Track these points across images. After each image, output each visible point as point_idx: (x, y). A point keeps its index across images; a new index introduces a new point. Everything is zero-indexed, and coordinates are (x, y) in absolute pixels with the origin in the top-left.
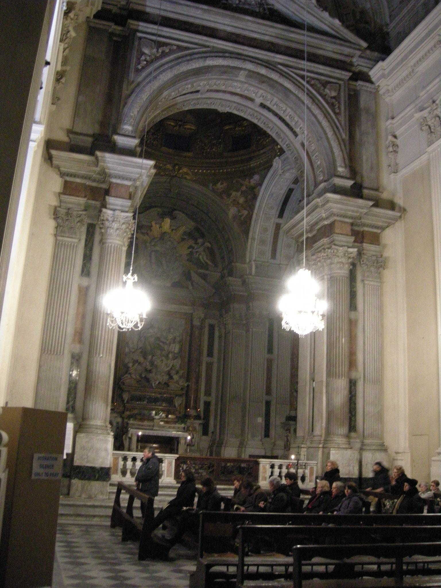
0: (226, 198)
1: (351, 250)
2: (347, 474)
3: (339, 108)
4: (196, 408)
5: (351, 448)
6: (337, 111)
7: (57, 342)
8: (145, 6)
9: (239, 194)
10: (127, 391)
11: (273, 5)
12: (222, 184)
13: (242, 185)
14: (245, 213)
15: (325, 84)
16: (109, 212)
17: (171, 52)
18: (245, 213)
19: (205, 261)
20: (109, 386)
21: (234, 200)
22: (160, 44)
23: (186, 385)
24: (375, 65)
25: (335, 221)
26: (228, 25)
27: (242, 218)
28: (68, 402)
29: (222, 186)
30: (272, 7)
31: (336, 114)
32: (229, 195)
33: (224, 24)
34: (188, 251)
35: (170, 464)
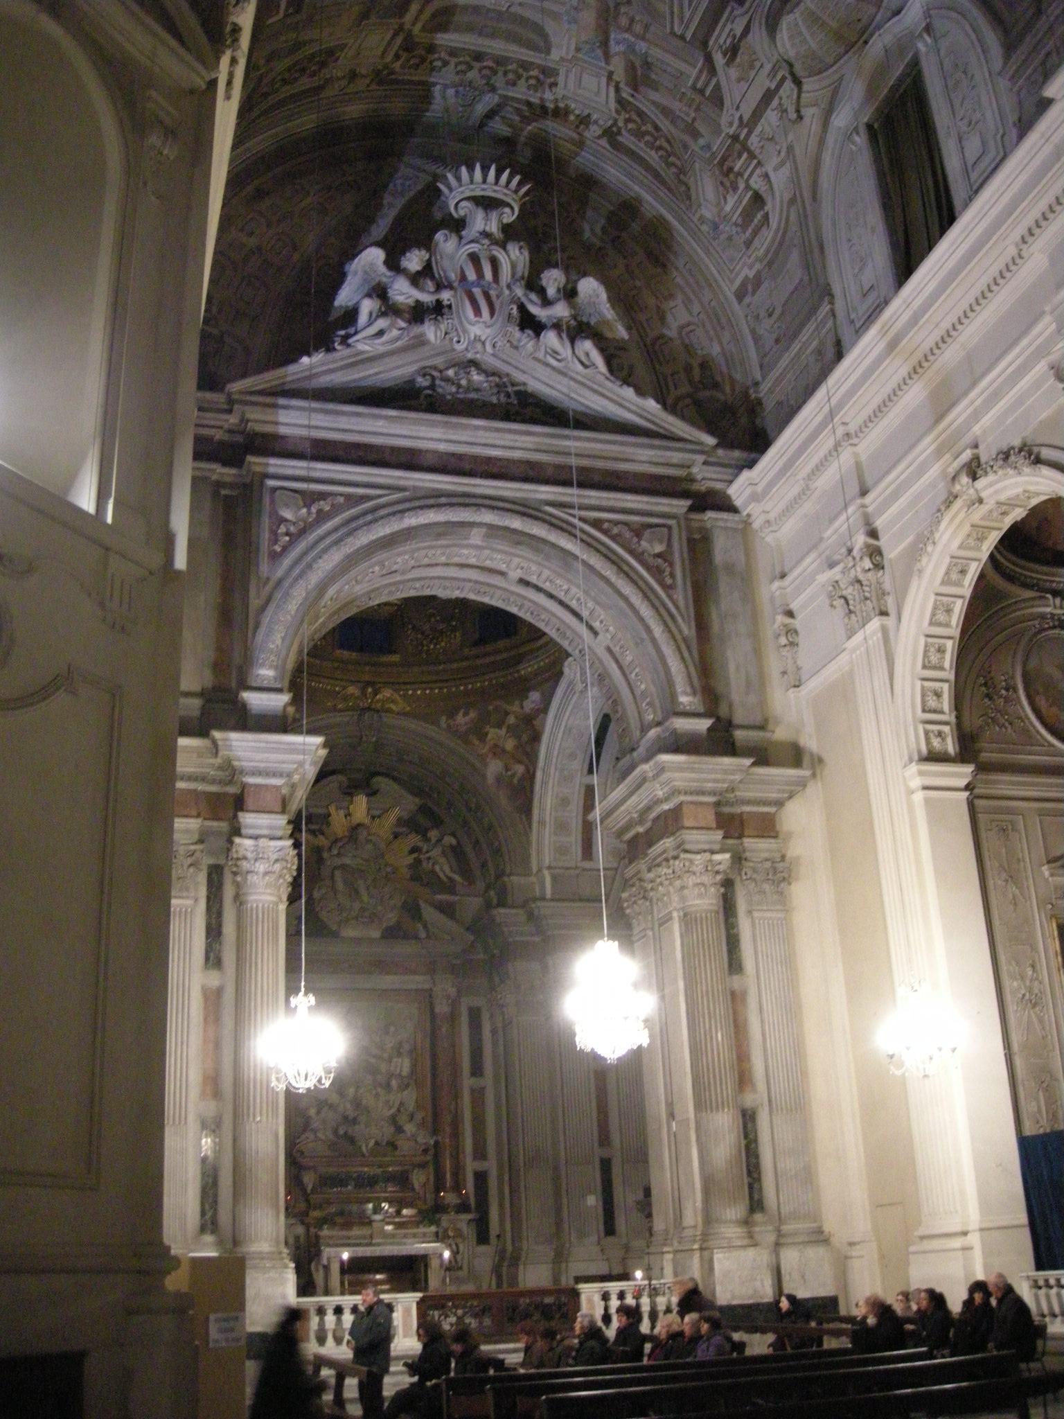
0: (477, 742)
1: (718, 857)
2: (750, 1298)
3: (672, 575)
4: (457, 1187)
5: (755, 1245)
6: (669, 581)
7: (178, 1106)
8: (277, 423)
9: (503, 732)
10: (309, 1168)
11: (524, 384)
12: (466, 714)
13: (507, 713)
14: (520, 769)
15: (638, 532)
16: (248, 843)
17: (336, 509)
18: (520, 769)
19: (447, 877)
20: (277, 1176)
21: (496, 746)
22: (310, 498)
23: (432, 1142)
24: (737, 475)
25: (680, 806)
26: (439, 440)
27: (515, 781)
28: (203, 1213)
29: (467, 718)
30: (521, 388)
31: (668, 588)
32: (482, 737)
33: (432, 439)
34: (410, 859)
35: (407, 1311)
